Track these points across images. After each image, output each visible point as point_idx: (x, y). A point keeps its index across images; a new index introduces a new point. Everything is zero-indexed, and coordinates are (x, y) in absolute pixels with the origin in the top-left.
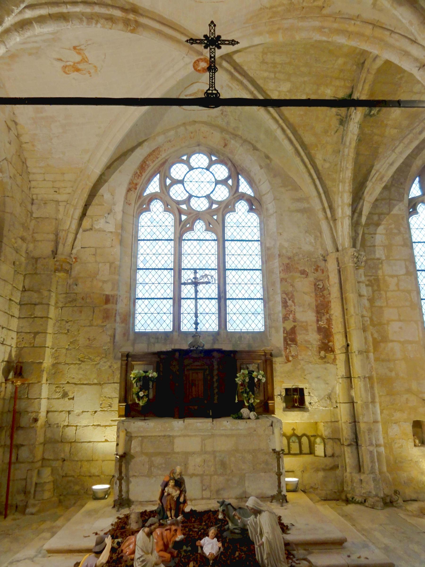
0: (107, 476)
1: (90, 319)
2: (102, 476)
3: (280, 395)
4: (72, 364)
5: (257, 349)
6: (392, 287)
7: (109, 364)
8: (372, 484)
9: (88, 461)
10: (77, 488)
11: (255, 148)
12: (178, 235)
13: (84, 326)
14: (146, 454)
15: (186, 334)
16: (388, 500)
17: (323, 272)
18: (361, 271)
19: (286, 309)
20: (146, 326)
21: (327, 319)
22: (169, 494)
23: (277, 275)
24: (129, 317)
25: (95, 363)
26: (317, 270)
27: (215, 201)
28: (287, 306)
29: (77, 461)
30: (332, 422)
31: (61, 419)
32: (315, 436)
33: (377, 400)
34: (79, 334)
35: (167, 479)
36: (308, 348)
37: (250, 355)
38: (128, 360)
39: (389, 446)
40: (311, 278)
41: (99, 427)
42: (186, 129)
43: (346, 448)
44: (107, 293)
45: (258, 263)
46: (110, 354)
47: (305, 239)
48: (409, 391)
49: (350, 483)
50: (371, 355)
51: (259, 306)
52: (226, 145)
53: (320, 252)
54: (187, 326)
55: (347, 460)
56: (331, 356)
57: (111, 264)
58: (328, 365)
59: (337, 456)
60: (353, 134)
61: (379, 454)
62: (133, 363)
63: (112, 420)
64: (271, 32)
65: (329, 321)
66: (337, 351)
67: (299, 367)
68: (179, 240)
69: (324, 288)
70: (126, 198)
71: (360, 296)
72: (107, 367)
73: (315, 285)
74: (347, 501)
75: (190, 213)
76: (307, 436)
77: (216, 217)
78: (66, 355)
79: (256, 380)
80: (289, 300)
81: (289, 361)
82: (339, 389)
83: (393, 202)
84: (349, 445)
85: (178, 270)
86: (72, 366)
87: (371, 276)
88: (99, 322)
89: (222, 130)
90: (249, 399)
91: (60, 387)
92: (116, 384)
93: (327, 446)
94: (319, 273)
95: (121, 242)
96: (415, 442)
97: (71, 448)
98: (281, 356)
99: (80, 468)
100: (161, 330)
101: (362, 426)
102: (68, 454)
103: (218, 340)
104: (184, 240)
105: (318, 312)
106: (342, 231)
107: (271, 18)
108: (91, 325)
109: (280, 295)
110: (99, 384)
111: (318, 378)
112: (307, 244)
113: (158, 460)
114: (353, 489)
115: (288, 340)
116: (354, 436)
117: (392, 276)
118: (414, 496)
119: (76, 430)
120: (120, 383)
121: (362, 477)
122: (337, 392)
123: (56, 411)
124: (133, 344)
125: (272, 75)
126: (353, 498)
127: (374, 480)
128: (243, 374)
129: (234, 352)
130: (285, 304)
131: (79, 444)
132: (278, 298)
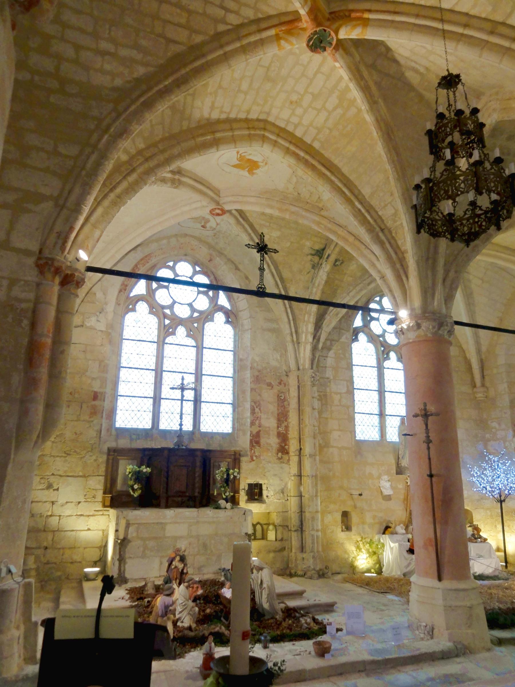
0: (89, 561)
1: (78, 414)
2: (84, 562)
3: (244, 489)
4: (58, 456)
5: (227, 449)
6: (336, 402)
7: (94, 457)
8: (311, 560)
9: (70, 548)
10: (59, 573)
11: (237, 268)
12: (162, 338)
13: (72, 421)
14: (142, 539)
15: (165, 433)
16: (321, 573)
17: (285, 386)
18: (315, 388)
19: (253, 415)
20: (126, 422)
21: (285, 426)
22: (176, 567)
23: (248, 385)
24: (112, 413)
25: (81, 456)
26: (280, 383)
27: (197, 310)
28: (255, 413)
29: (60, 549)
30: (283, 512)
31: (45, 509)
32: (268, 524)
33: (319, 494)
34: (66, 428)
35: (173, 556)
36: (269, 450)
37: (222, 454)
38: (114, 455)
39: (324, 531)
40: (275, 391)
41: (82, 517)
42: (178, 240)
43: (293, 533)
44: (95, 390)
45: (230, 372)
46: (96, 448)
47: (273, 356)
48: (341, 487)
49: (294, 561)
50: (318, 458)
51: (229, 409)
52: (210, 260)
53: (284, 368)
55: (293, 543)
56: (286, 457)
57: (101, 362)
58: (284, 464)
59: (286, 540)
60: (322, 280)
61: (317, 537)
62: (118, 457)
63: (95, 511)
64: (280, 210)
65: (287, 427)
66: (291, 453)
67: (261, 465)
68: (161, 343)
69: (284, 400)
70: (117, 299)
71: (314, 409)
72: (92, 461)
73: (278, 396)
74: (291, 575)
75: (174, 319)
76: (261, 525)
77: (196, 325)
78: (52, 447)
79: (232, 477)
80: (257, 407)
81: (253, 460)
82: (291, 485)
83: (343, 331)
84: (295, 531)
85: (159, 372)
86: (58, 459)
87: (321, 392)
88: (87, 418)
89: (210, 246)
90: (226, 492)
91: (45, 478)
92: (101, 477)
93: (278, 532)
94: (282, 387)
95: (110, 342)
96: (342, 528)
97: (54, 536)
98: (247, 455)
99: (63, 555)
100: (141, 427)
101: (307, 515)
102: (51, 542)
103: (193, 439)
104: (167, 343)
105: (279, 420)
106: (304, 354)
107: (281, 199)
108: (78, 420)
109: (249, 403)
110: (84, 476)
111: (275, 475)
112: (274, 360)
113: (151, 544)
114: (296, 566)
115: (254, 443)
116: (300, 523)
117: (336, 393)
118: (338, 570)
119: (59, 520)
120: (106, 476)
121: (304, 555)
122: (289, 487)
123: (40, 502)
124: (116, 440)
125: (268, 224)
126: (296, 573)
127: (313, 557)
128: (222, 471)
129: (209, 451)
130: (253, 412)
131: (62, 533)
132: (248, 405)
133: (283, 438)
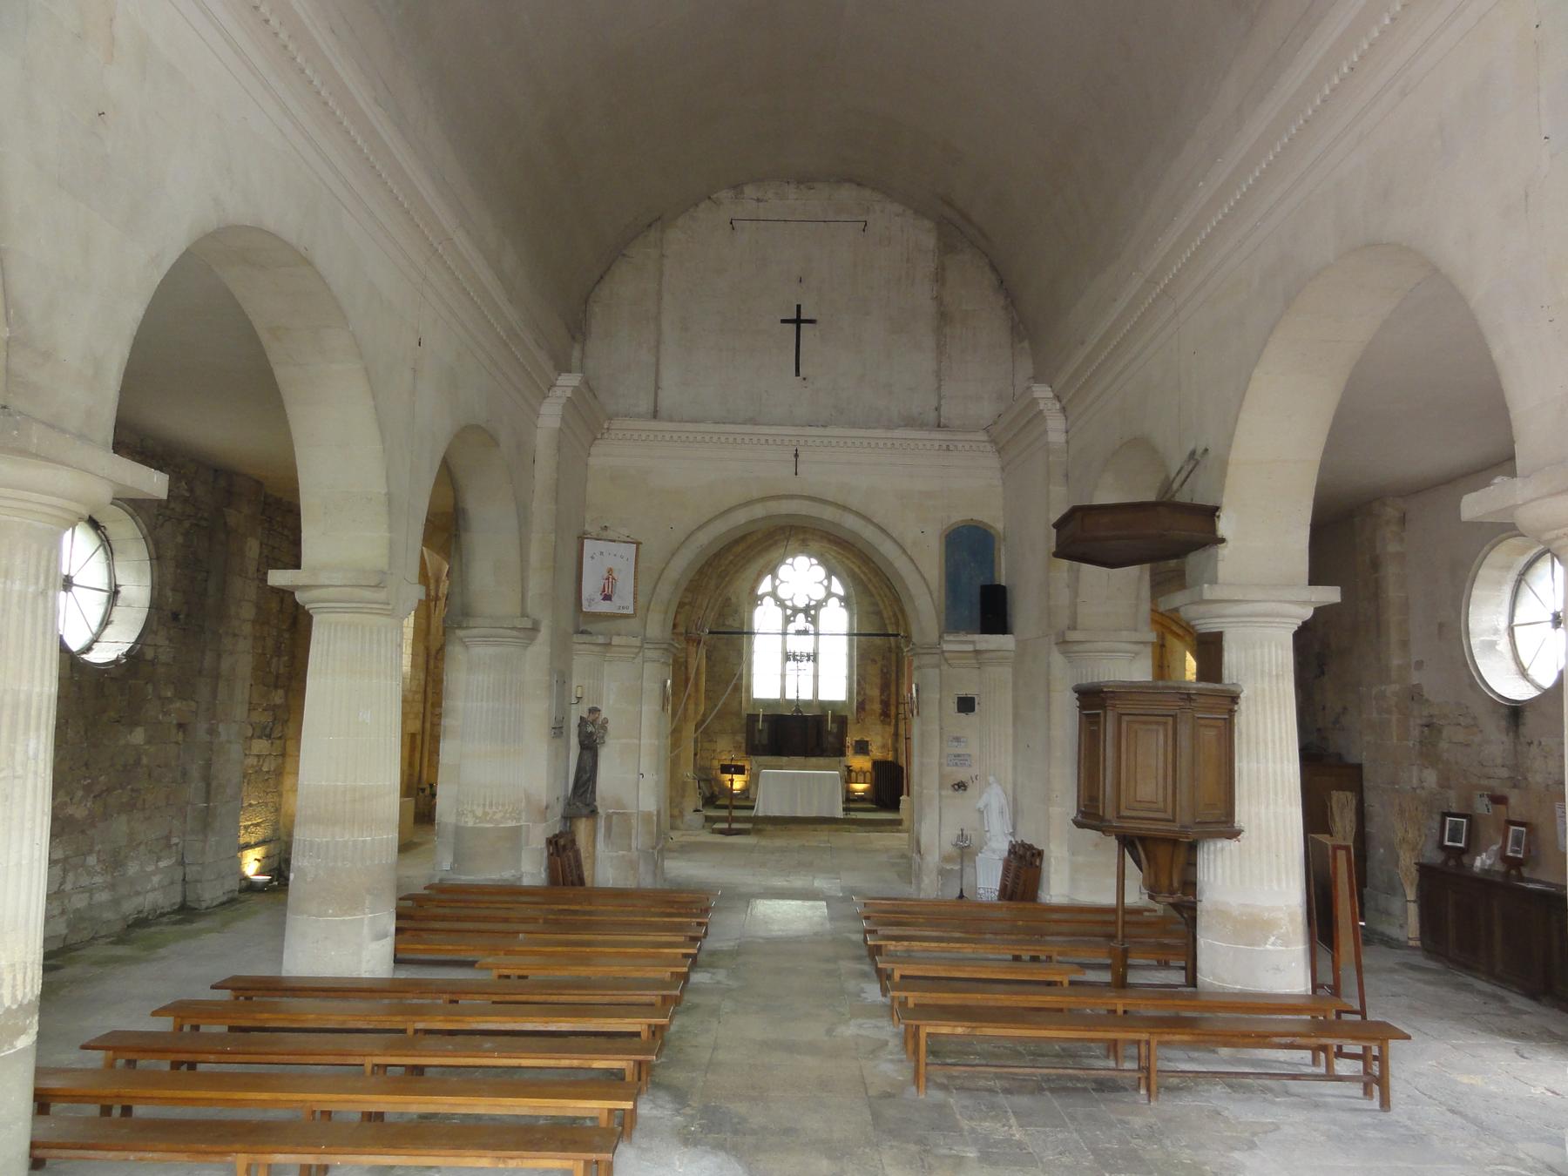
15: (790, 702)
54: (791, 695)
133: (885, 704)
